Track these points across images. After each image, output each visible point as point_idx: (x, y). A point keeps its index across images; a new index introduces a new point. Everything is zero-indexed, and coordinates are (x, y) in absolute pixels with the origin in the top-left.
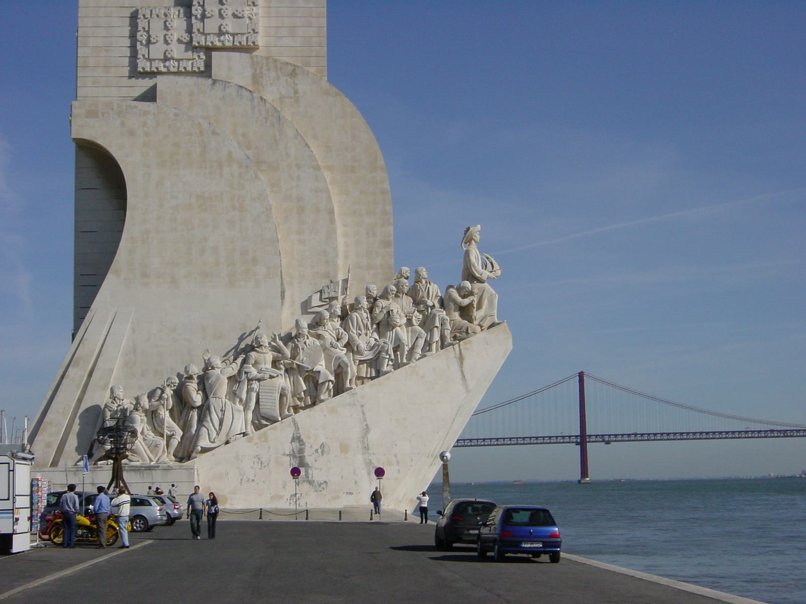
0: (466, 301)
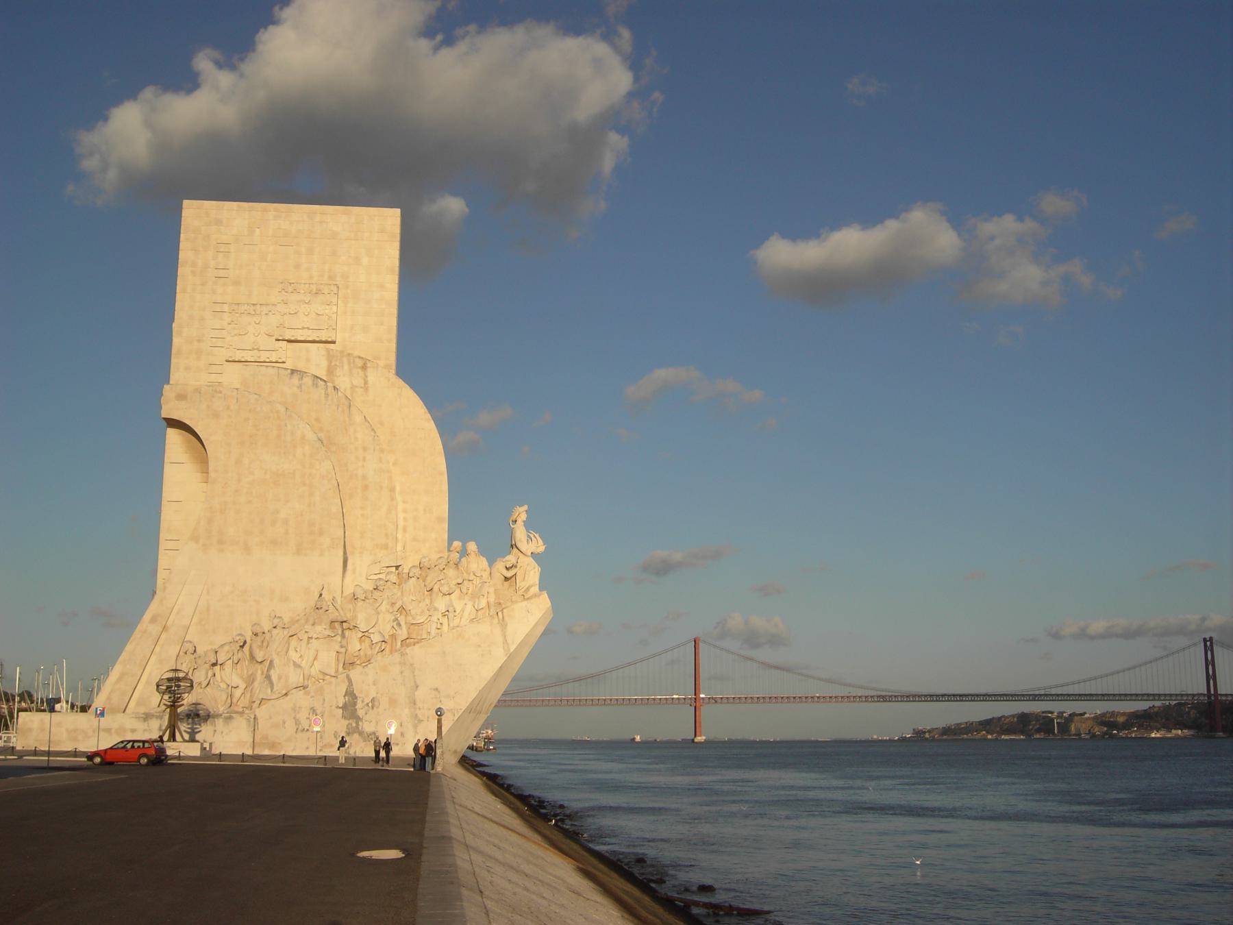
0: (509, 574)
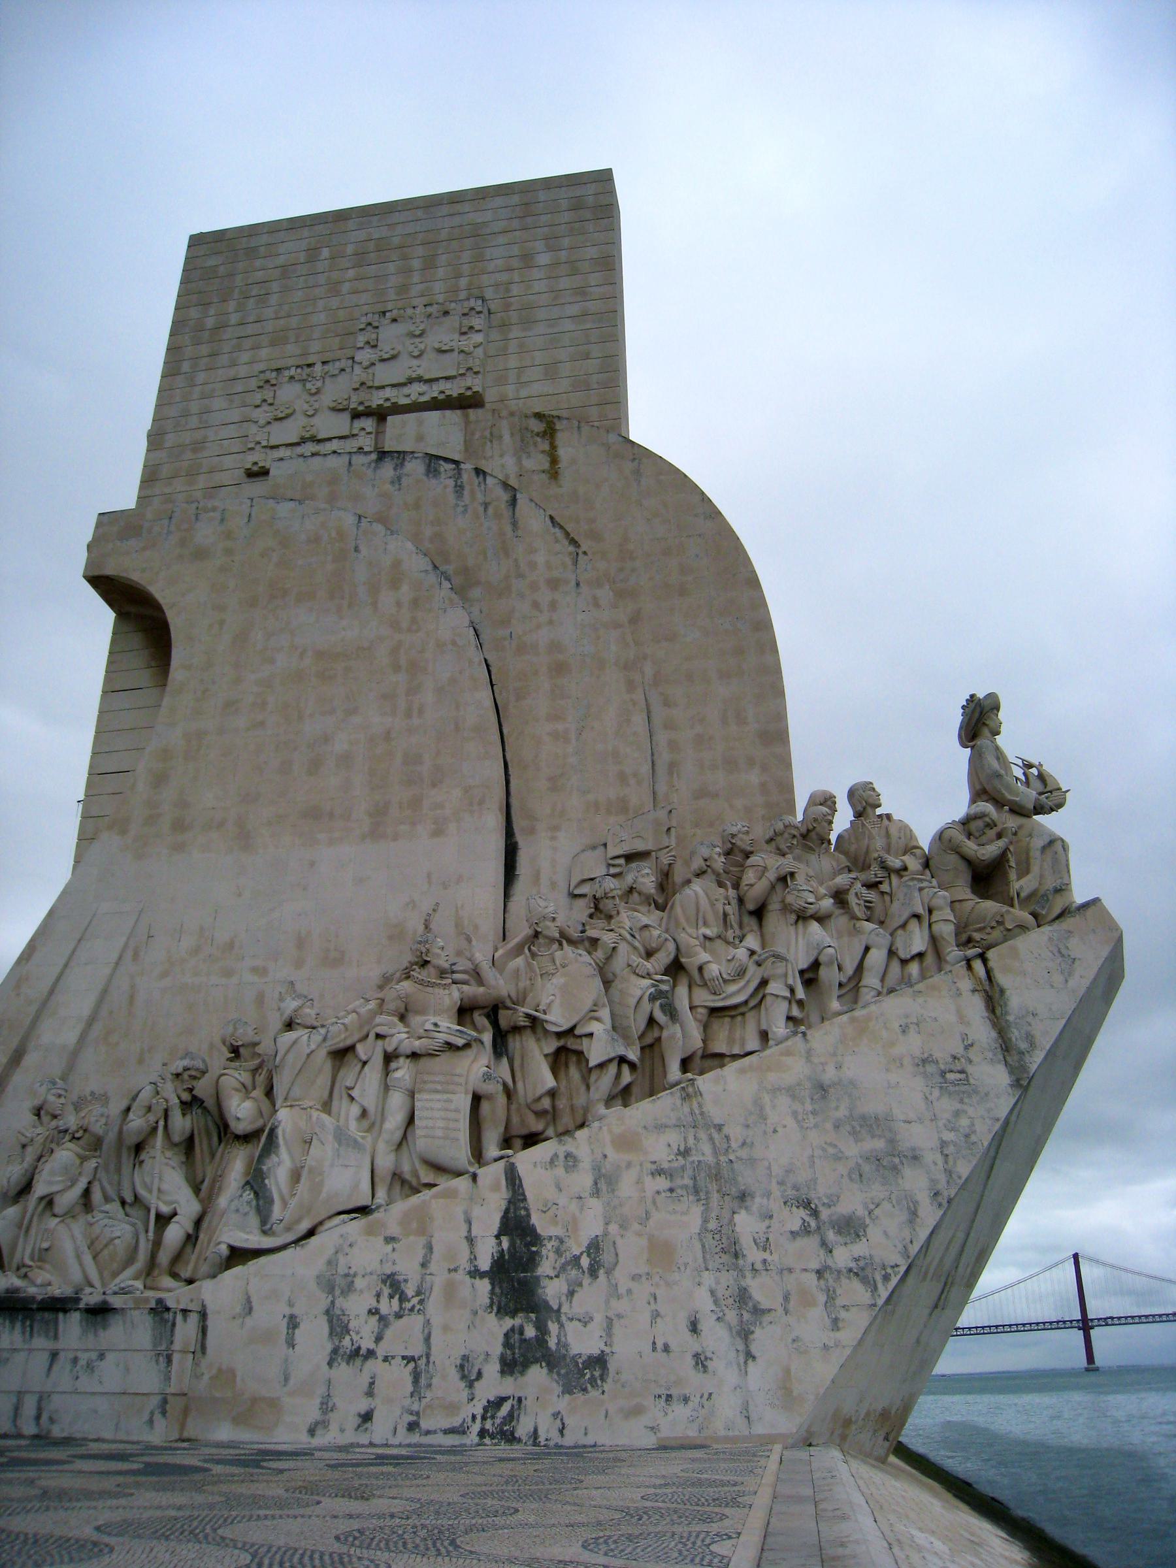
0: (990, 851)
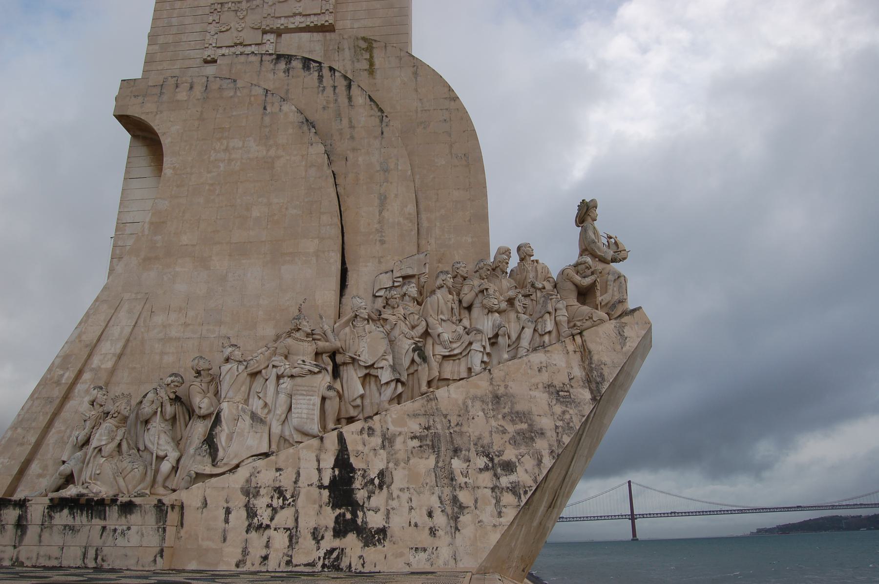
0: (587, 281)
